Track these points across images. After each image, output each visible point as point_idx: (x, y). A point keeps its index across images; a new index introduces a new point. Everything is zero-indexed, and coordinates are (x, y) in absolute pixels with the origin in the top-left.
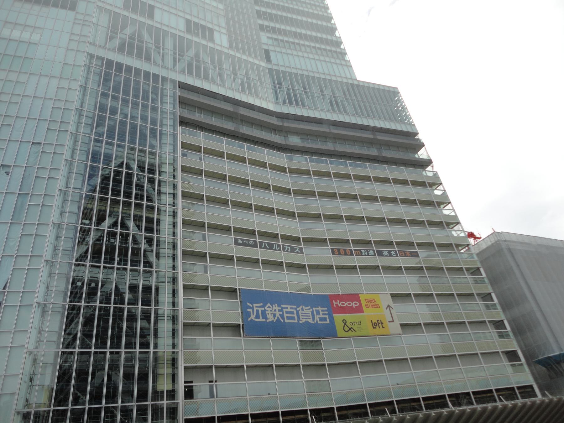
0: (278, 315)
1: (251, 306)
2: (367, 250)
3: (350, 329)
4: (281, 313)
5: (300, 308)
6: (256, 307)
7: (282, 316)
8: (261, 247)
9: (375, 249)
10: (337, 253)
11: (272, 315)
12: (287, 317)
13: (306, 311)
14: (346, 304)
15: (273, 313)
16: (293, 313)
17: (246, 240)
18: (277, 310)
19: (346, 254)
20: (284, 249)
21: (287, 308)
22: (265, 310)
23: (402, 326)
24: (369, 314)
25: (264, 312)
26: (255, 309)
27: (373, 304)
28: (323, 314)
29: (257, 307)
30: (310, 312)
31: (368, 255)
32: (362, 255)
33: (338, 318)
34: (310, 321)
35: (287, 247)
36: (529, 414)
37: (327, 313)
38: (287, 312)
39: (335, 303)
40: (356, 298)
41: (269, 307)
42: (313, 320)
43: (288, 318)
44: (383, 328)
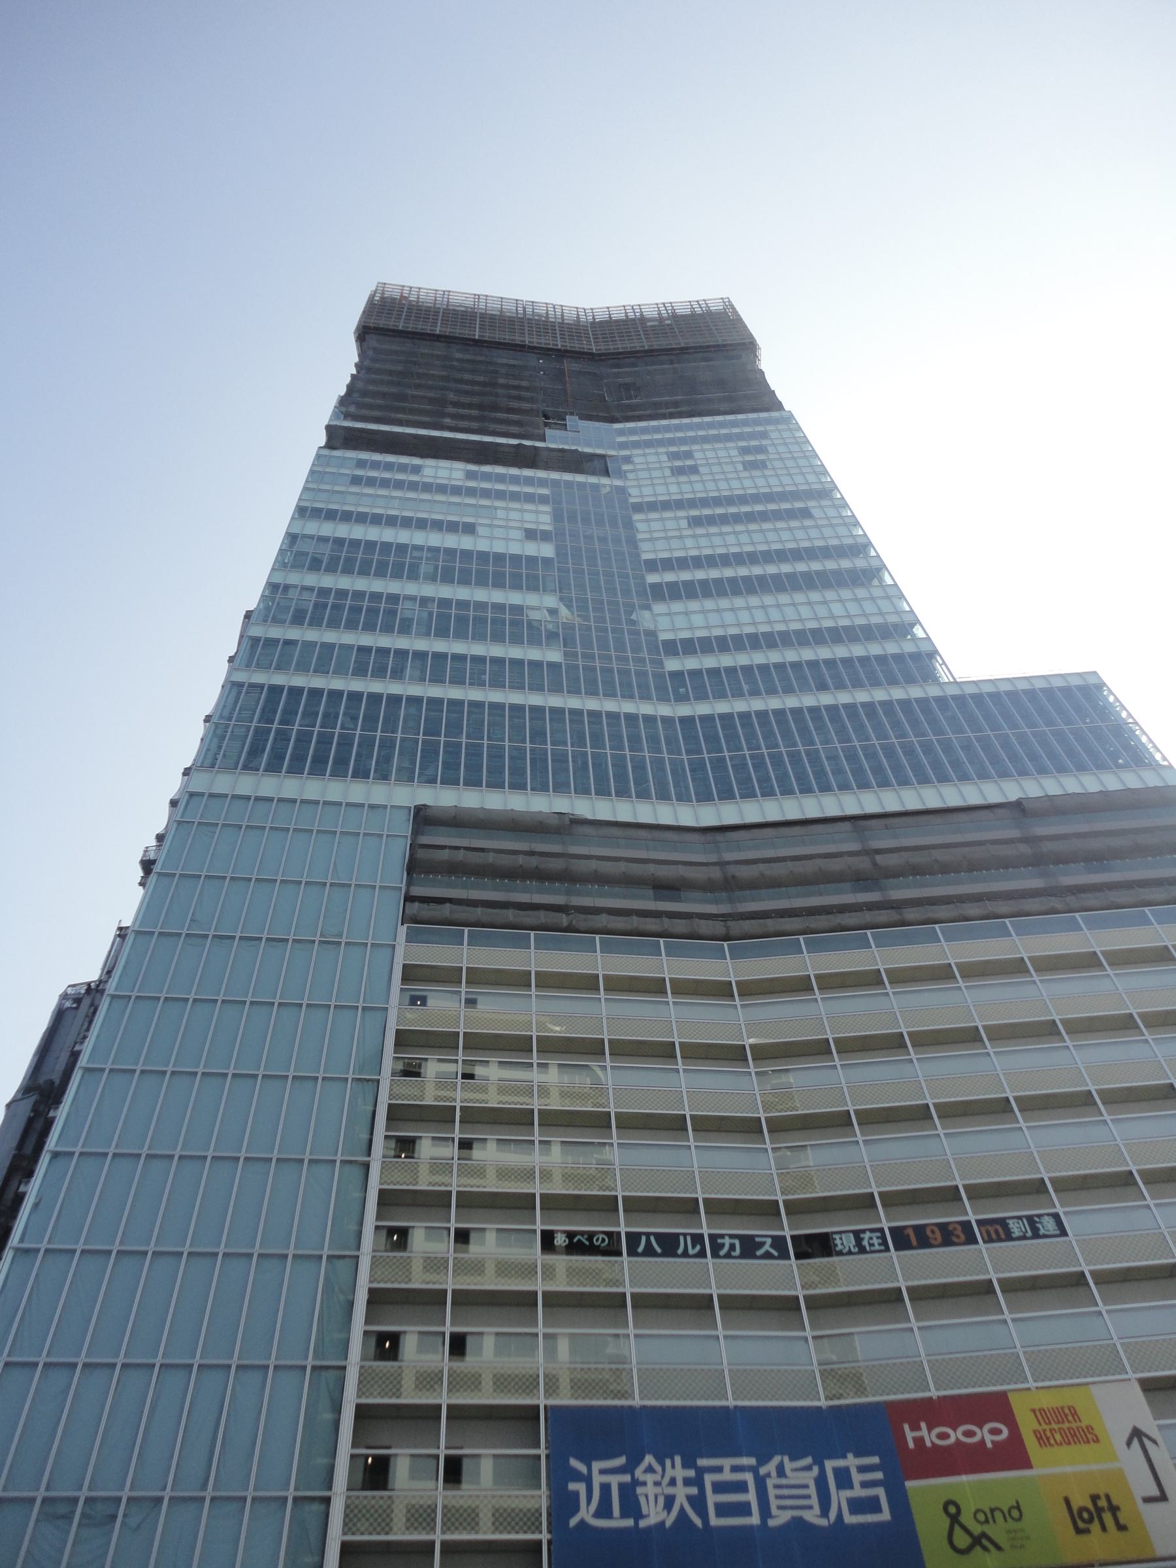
0: (681, 1500)
1: (582, 1468)
2: (1030, 1219)
3: (978, 1541)
4: (694, 1491)
5: (771, 1467)
6: (603, 1472)
7: (698, 1503)
8: (632, 1252)
9: (885, 1225)
10: (963, 1237)
11: (661, 1500)
13: (793, 1478)
14: (956, 1435)
16: (741, 1487)
17: (582, 1233)
18: (679, 1482)
20: (716, 1249)
21: (719, 1469)
22: (636, 1483)
24: (1056, 1469)
25: (629, 1493)
26: (597, 1480)
27: (1070, 1428)
28: (865, 1485)
29: (604, 1473)
31: (1036, 1235)
32: (1009, 1237)
34: (812, 1516)
35: (727, 1241)
37: (879, 1475)
38: (719, 1488)
39: (910, 1435)
41: (650, 1469)
42: (825, 1512)
44: (1121, 1528)
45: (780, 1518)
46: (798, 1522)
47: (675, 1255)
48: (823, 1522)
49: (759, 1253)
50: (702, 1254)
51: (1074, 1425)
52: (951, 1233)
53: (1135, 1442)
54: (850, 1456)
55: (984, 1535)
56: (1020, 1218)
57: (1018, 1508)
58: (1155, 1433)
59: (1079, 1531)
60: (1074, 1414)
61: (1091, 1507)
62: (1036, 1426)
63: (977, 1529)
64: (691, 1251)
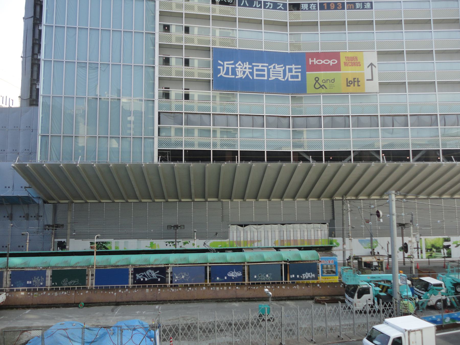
1: (222, 63)
3: (321, 86)
4: (251, 70)
5: (272, 66)
6: (227, 64)
7: (252, 73)
11: (242, 72)
12: (256, 74)
13: (277, 69)
15: (242, 70)
16: (263, 70)
18: (247, 68)
19: (336, 8)
21: (258, 66)
23: (380, 84)
24: (348, 71)
26: (226, 66)
27: (354, 62)
28: (296, 72)
29: (228, 65)
30: (282, 70)
31: (363, 8)
32: (355, 8)
33: (311, 75)
35: (269, 4)
37: (300, 70)
38: (257, 70)
39: (310, 61)
40: (336, 56)
41: (240, 65)
42: (284, 78)
43: (257, 75)
44: (359, 86)
45: (272, 78)
46: (277, 79)
47: (253, 7)
48: (284, 80)
49: (278, 8)
50: (260, 7)
52: (338, 6)
53: (370, 67)
54: (293, 65)
55: (323, 85)
56: (360, 2)
57: (334, 80)
58: (376, 65)
59: (347, 86)
60: (356, 58)
61: (353, 80)
63: (322, 84)
64: (257, 6)
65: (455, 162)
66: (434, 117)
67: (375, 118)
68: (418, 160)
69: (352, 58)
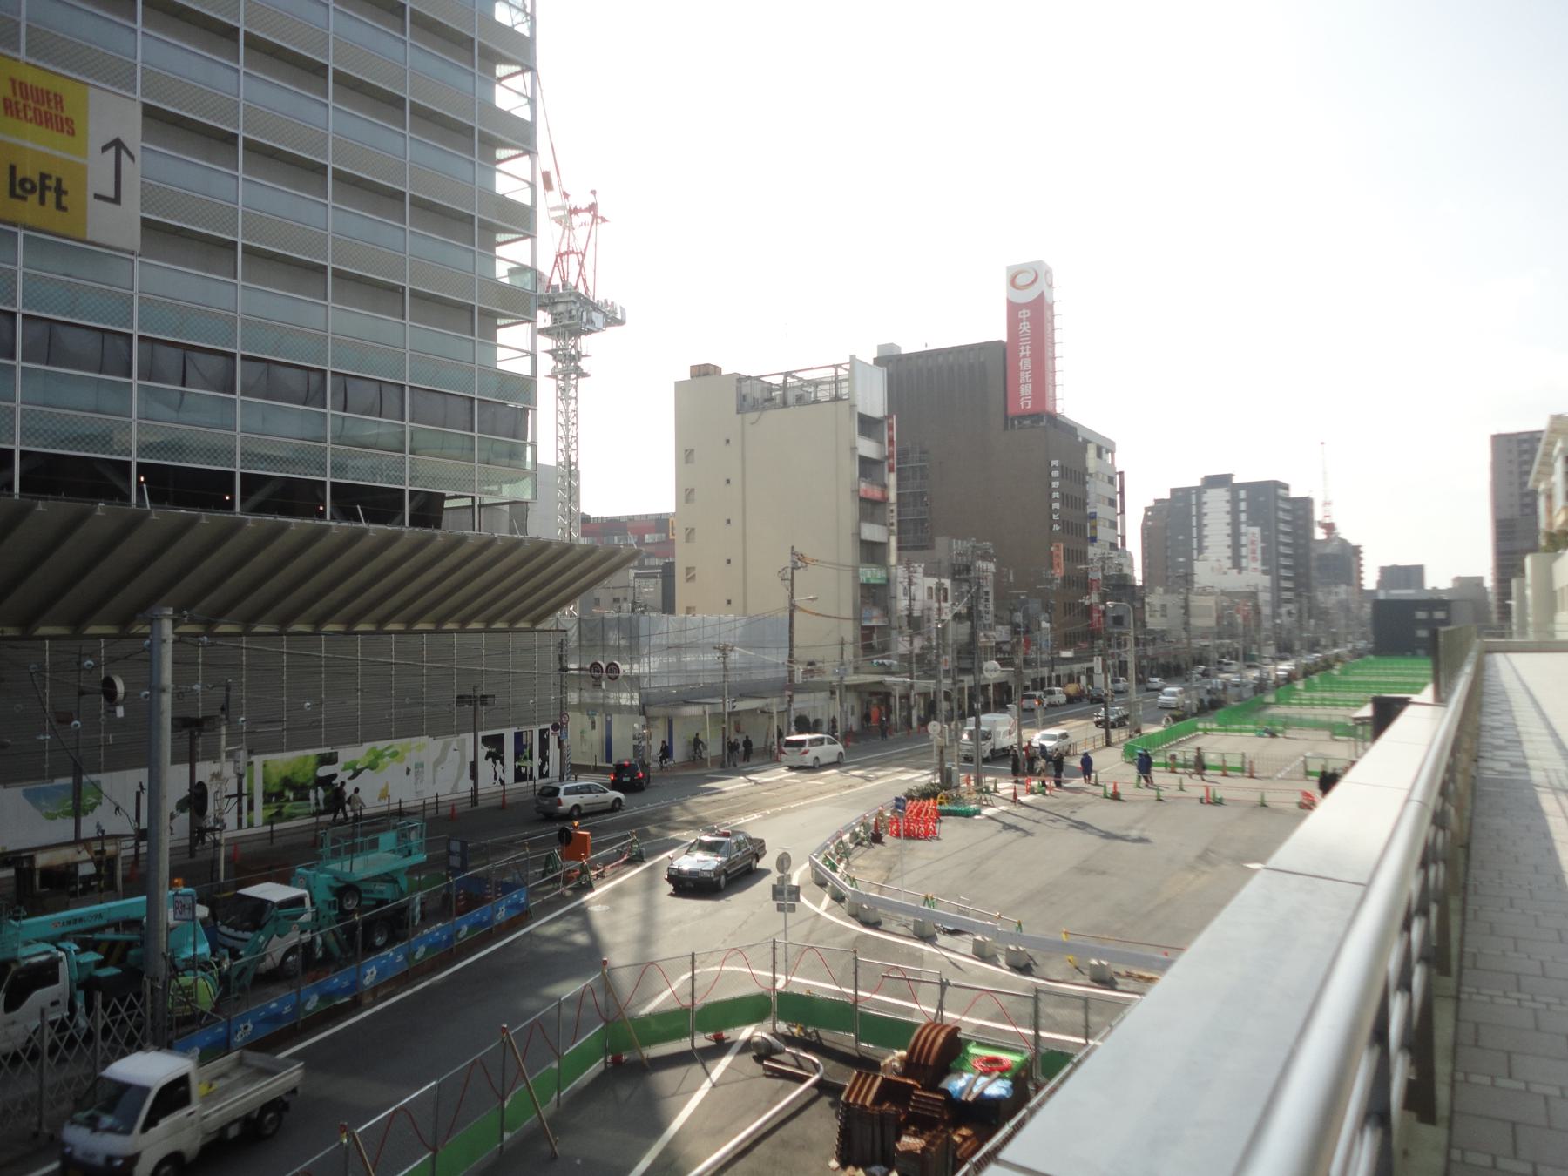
23: (146, 223)
36: (406, 567)
44: (60, 206)
51: (53, 112)
53: (112, 150)
58: (137, 153)
59: (13, 194)
60: (59, 101)
61: (36, 179)
62: (9, 94)
65: (364, 525)
66: (314, 378)
67: (120, 342)
68: (259, 509)
69: (42, 96)
